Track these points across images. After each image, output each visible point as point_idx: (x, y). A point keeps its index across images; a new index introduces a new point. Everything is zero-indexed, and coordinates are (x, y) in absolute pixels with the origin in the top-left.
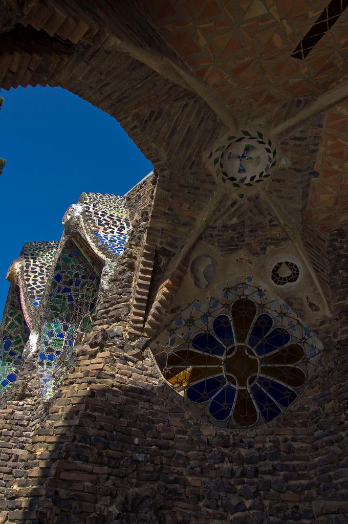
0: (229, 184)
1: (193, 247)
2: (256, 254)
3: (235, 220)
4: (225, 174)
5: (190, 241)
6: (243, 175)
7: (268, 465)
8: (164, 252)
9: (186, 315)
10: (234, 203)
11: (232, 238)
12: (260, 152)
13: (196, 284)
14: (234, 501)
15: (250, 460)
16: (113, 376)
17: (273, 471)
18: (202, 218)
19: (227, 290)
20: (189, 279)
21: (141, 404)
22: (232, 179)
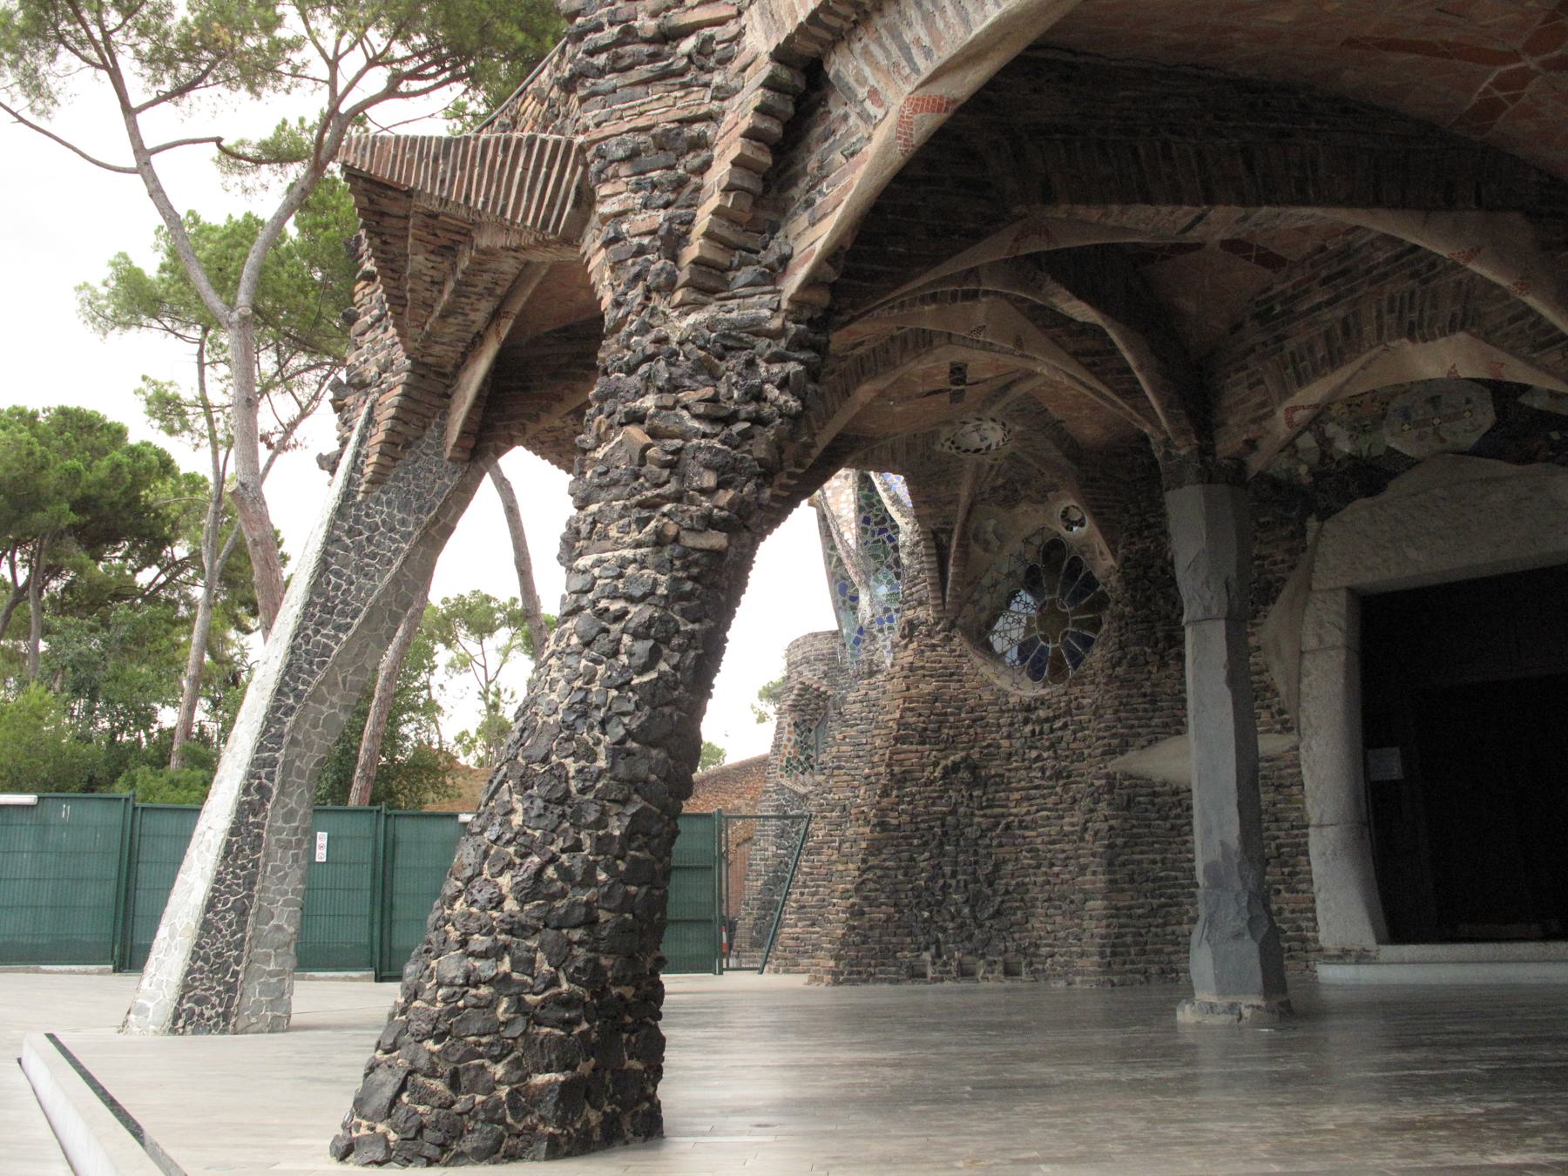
0: (976, 456)
1: (967, 520)
2: (1041, 503)
3: (1000, 481)
4: (967, 451)
5: (961, 515)
6: (987, 443)
7: (1058, 724)
8: (943, 531)
9: (986, 581)
10: (992, 467)
11: (1006, 496)
12: (988, 425)
13: (986, 550)
14: (1034, 754)
15: (1047, 720)
16: (923, 667)
17: (1065, 726)
18: (964, 494)
19: (1027, 541)
20: (976, 550)
21: (953, 685)
22: (977, 451)
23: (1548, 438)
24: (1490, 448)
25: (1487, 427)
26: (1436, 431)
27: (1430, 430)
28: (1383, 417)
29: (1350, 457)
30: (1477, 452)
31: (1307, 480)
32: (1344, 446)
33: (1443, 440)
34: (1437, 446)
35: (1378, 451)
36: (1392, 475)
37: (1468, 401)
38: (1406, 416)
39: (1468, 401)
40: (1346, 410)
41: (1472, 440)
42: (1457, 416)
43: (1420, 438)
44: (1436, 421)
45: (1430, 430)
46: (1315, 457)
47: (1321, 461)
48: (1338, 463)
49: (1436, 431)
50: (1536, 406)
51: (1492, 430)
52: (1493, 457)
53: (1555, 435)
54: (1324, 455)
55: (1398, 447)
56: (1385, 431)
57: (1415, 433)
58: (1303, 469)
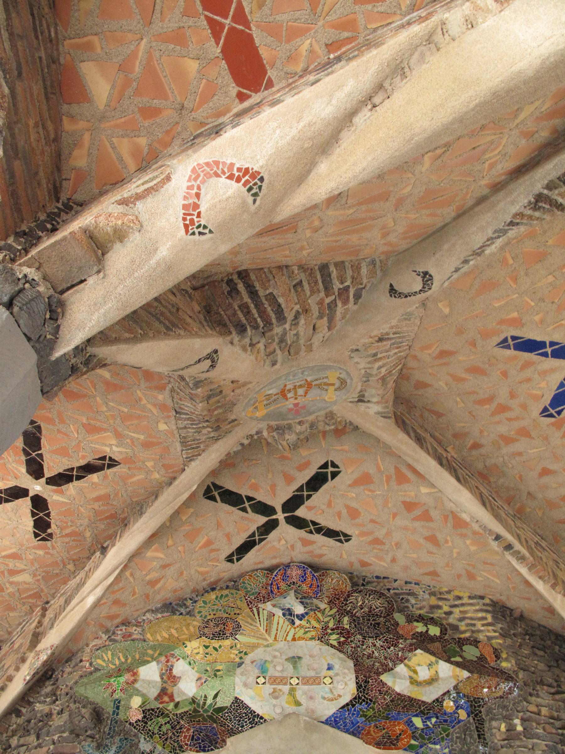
23: (410, 723)
24: (346, 720)
25: (346, 699)
26: (292, 692)
27: (286, 688)
28: (240, 665)
29: (193, 701)
30: (334, 722)
31: (135, 716)
32: (188, 687)
33: (298, 704)
34: (291, 708)
35: (224, 701)
36: (232, 733)
37: (329, 669)
38: (263, 670)
39: (329, 669)
40: (201, 650)
41: (329, 709)
42: (316, 681)
43: (275, 695)
44: (294, 681)
45: (286, 688)
46: (153, 692)
47: (159, 697)
48: (177, 705)
49: (292, 692)
50: (398, 689)
51: (351, 704)
52: (353, 734)
53: (418, 722)
54: (163, 692)
55: (248, 701)
56: (238, 680)
57: (269, 688)
58: (136, 702)
